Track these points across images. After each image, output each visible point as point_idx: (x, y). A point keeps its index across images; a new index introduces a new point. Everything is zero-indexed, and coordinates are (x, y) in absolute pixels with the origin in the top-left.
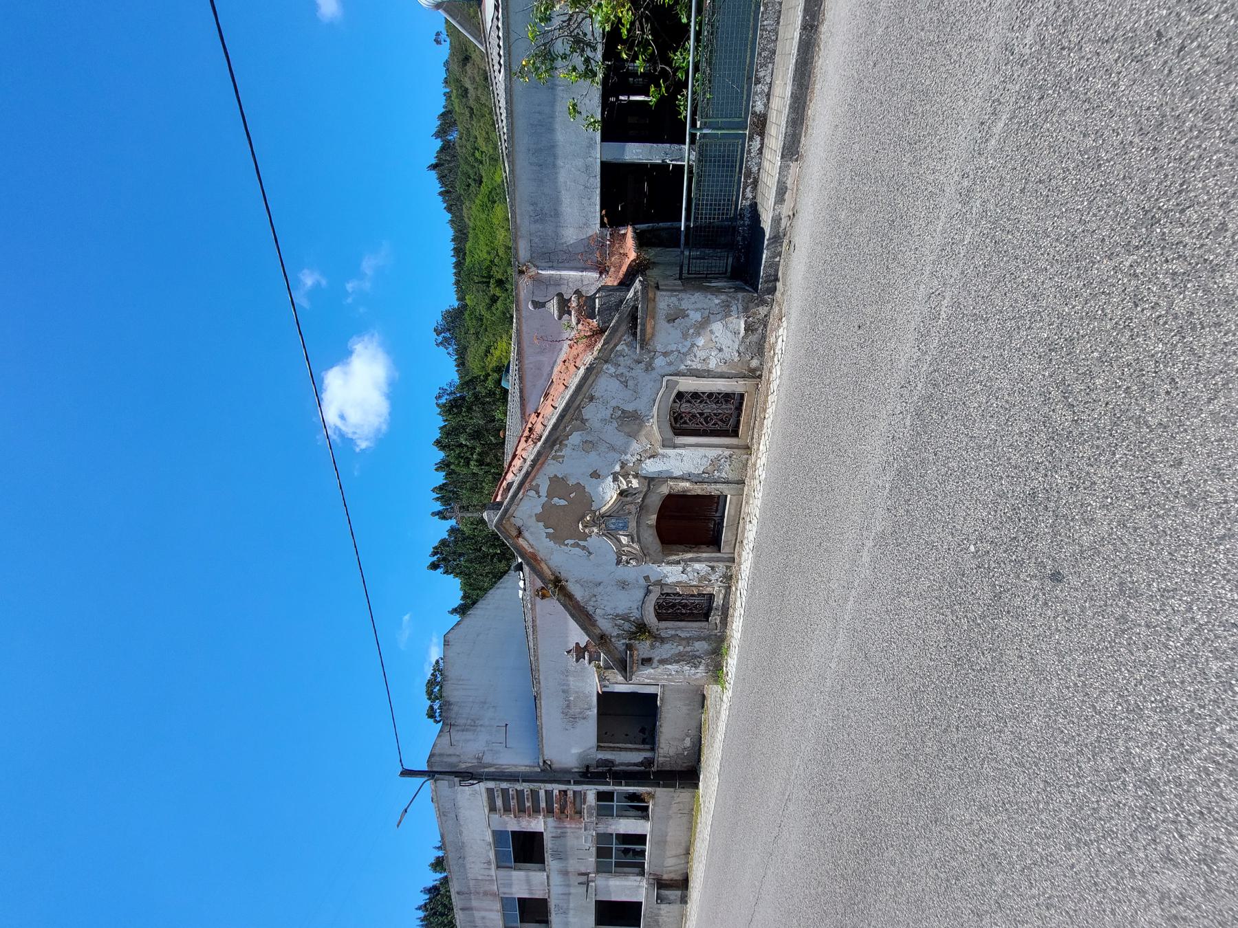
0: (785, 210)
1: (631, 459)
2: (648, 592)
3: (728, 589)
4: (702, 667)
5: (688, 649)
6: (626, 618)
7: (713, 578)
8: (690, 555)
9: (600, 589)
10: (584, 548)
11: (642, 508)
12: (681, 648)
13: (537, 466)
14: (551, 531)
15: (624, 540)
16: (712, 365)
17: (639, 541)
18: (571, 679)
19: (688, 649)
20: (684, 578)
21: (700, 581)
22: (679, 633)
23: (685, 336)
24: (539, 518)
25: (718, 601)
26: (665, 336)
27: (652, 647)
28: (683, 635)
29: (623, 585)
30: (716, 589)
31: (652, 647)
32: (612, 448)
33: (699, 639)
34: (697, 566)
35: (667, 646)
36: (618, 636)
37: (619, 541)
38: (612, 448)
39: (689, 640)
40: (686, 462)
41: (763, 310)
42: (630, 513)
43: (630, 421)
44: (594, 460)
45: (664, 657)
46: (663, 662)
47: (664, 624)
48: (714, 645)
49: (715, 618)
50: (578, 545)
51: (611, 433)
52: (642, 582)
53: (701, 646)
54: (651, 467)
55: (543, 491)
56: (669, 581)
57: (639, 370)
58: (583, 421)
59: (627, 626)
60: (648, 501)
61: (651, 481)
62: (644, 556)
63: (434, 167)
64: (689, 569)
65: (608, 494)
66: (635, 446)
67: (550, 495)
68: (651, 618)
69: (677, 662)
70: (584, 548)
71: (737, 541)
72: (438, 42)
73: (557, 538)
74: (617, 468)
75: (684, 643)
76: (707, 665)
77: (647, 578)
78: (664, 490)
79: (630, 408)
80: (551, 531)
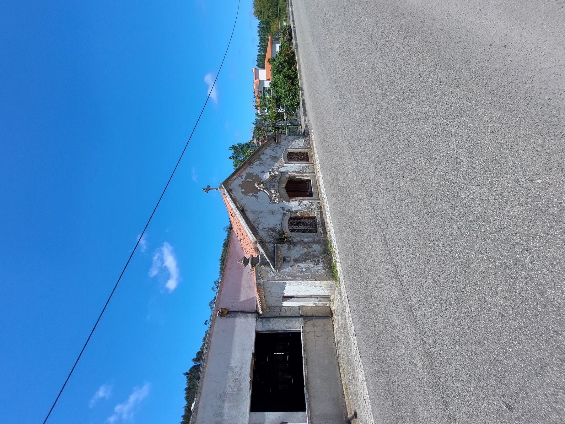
0: (307, 122)
1: (275, 168)
2: (284, 214)
3: (321, 212)
4: (321, 265)
5: (310, 250)
6: (273, 230)
7: (313, 207)
8: (301, 198)
9: (262, 215)
10: (256, 196)
11: (280, 182)
12: (305, 249)
13: (244, 167)
14: (243, 190)
15: (273, 191)
16: (297, 147)
17: (279, 193)
18: (226, 405)
19: (310, 250)
20: (300, 208)
21: (307, 209)
22: (302, 239)
23: (289, 142)
24: (240, 186)
25: (318, 219)
26: (283, 142)
27: (289, 249)
28: (305, 240)
29: (272, 212)
30: (315, 213)
31: (289, 249)
32: (269, 165)
33: (314, 242)
34: (305, 202)
35: (297, 248)
36: (269, 242)
37: (271, 192)
38: (269, 165)
39: (308, 244)
40: (293, 168)
41: (308, 138)
42: (275, 182)
43: (275, 159)
44: (263, 168)
45: (297, 256)
46: (297, 260)
47: (293, 234)
48: (324, 247)
49: (320, 229)
50: (253, 195)
51: (269, 161)
52: (281, 210)
53: (317, 248)
54: (282, 170)
55: (244, 177)
56: (293, 210)
57: (277, 148)
58: (260, 159)
59: (274, 234)
60: (282, 179)
61: (282, 174)
62: (281, 198)
63: (187, 374)
64: (301, 204)
65: (267, 176)
66: (276, 164)
67: (246, 179)
68: (286, 228)
69: (305, 260)
70: (256, 196)
71: (317, 186)
72: (205, 324)
73: (245, 193)
74: (271, 170)
75: (306, 245)
76: (324, 263)
77: (283, 208)
78: (287, 176)
79: (275, 156)
80: (243, 190)
